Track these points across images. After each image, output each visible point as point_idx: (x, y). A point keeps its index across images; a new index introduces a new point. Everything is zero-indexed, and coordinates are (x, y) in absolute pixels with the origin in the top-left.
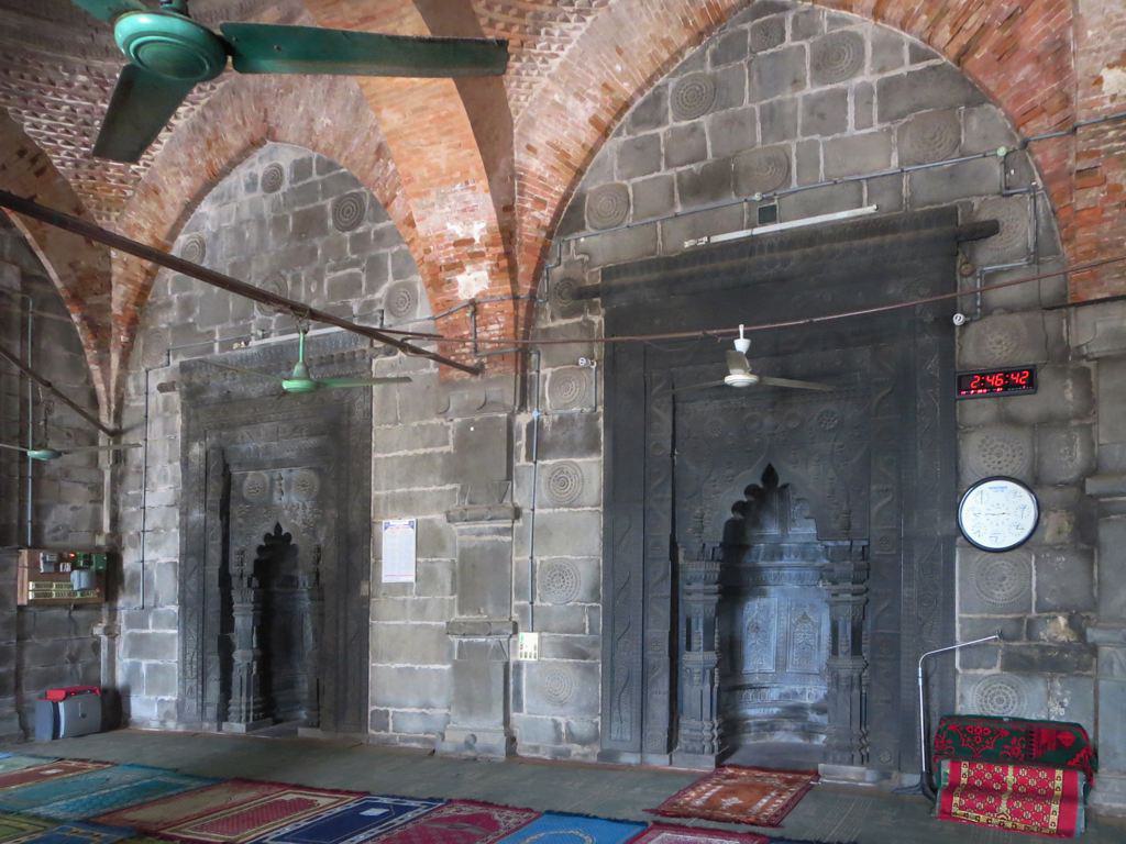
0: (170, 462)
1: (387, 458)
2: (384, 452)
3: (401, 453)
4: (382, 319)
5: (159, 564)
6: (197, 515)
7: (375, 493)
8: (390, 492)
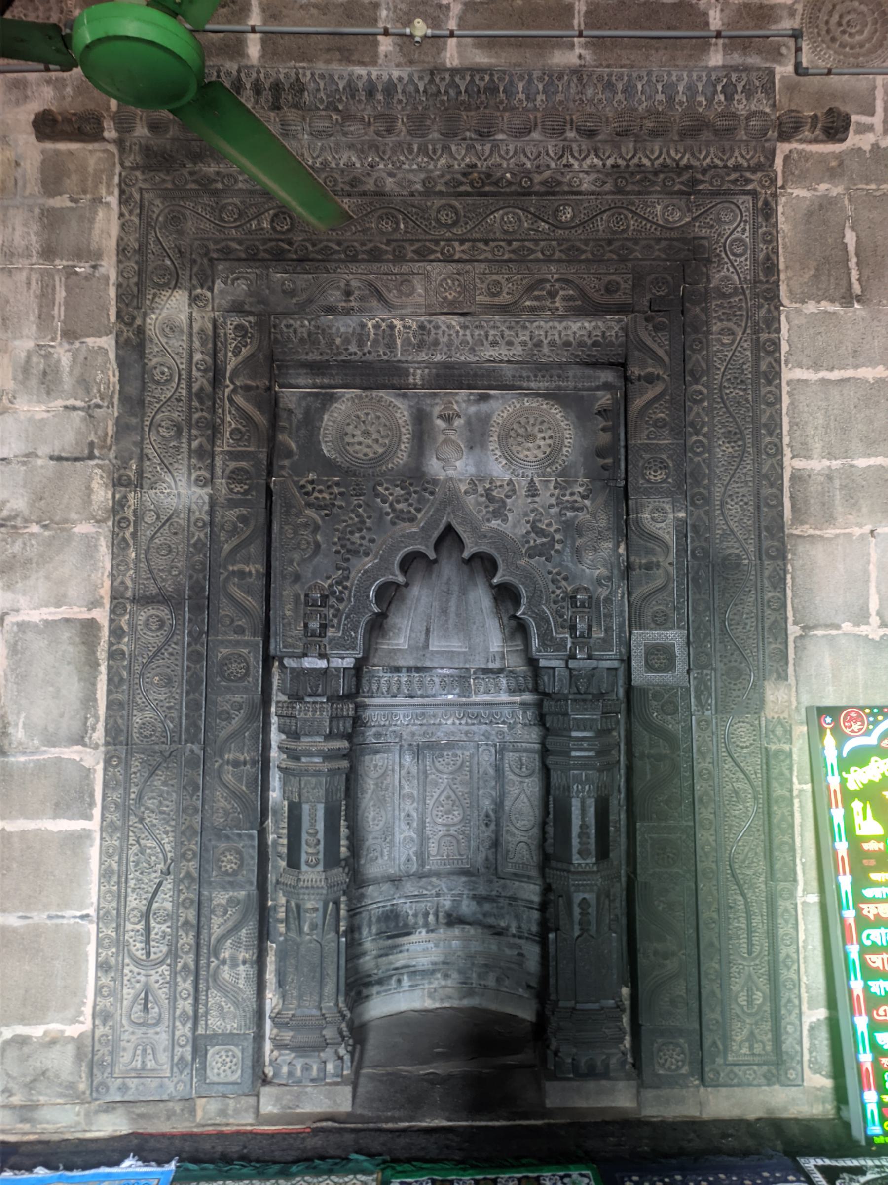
0: (70, 335)
1: (824, 382)
2: (816, 366)
3: (868, 373)
4: (798, 50)
5: (22, 626)
6: (181, 491)
7: (791, 464)
8: (836, 464)
